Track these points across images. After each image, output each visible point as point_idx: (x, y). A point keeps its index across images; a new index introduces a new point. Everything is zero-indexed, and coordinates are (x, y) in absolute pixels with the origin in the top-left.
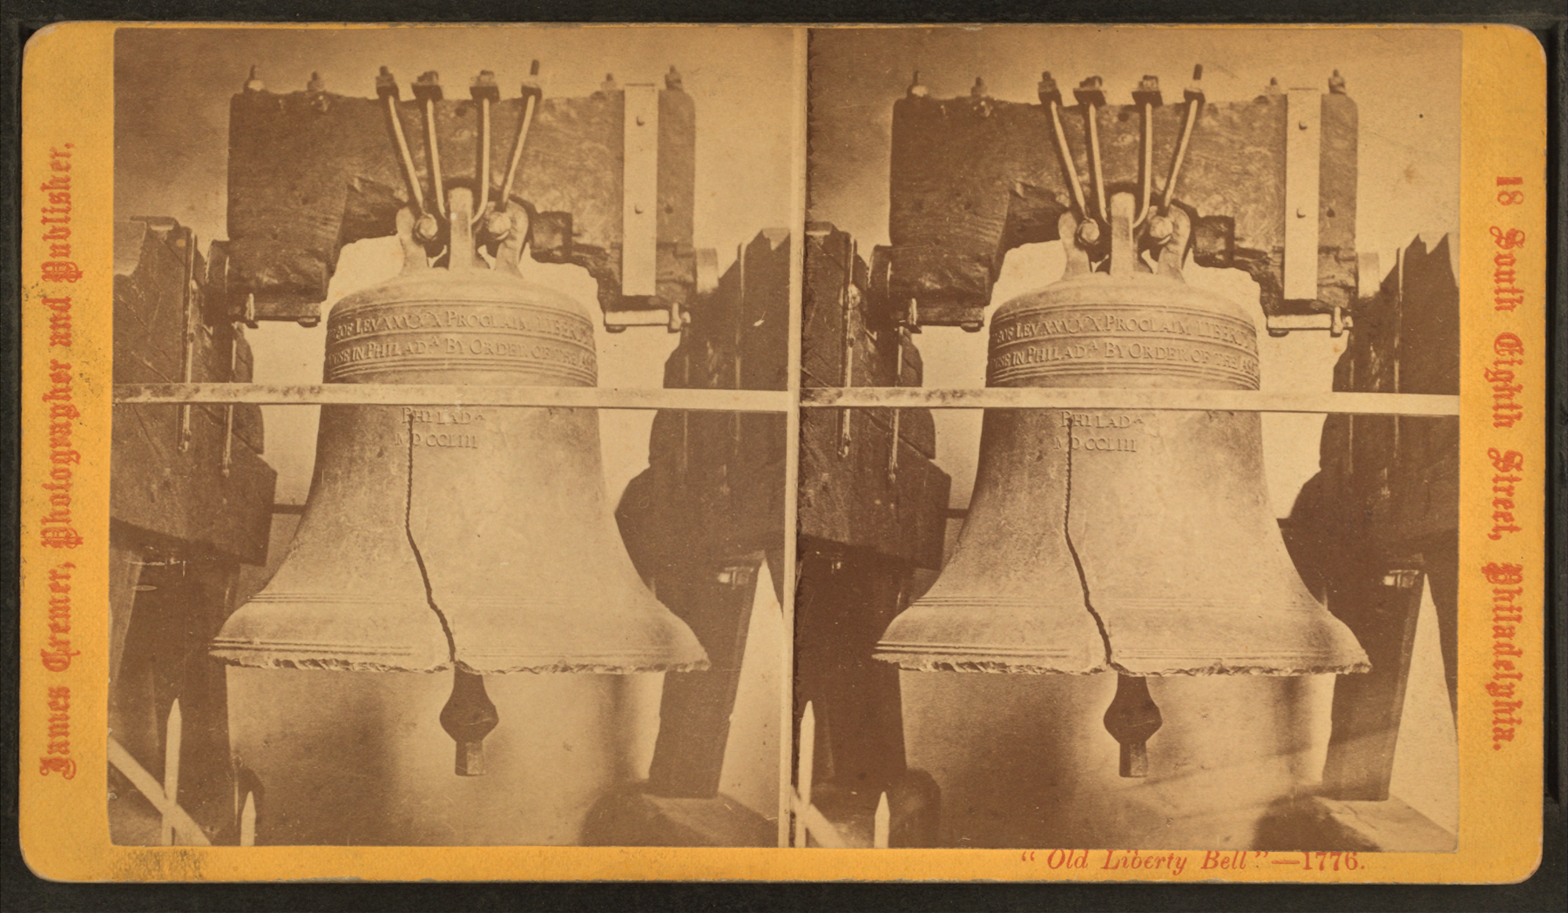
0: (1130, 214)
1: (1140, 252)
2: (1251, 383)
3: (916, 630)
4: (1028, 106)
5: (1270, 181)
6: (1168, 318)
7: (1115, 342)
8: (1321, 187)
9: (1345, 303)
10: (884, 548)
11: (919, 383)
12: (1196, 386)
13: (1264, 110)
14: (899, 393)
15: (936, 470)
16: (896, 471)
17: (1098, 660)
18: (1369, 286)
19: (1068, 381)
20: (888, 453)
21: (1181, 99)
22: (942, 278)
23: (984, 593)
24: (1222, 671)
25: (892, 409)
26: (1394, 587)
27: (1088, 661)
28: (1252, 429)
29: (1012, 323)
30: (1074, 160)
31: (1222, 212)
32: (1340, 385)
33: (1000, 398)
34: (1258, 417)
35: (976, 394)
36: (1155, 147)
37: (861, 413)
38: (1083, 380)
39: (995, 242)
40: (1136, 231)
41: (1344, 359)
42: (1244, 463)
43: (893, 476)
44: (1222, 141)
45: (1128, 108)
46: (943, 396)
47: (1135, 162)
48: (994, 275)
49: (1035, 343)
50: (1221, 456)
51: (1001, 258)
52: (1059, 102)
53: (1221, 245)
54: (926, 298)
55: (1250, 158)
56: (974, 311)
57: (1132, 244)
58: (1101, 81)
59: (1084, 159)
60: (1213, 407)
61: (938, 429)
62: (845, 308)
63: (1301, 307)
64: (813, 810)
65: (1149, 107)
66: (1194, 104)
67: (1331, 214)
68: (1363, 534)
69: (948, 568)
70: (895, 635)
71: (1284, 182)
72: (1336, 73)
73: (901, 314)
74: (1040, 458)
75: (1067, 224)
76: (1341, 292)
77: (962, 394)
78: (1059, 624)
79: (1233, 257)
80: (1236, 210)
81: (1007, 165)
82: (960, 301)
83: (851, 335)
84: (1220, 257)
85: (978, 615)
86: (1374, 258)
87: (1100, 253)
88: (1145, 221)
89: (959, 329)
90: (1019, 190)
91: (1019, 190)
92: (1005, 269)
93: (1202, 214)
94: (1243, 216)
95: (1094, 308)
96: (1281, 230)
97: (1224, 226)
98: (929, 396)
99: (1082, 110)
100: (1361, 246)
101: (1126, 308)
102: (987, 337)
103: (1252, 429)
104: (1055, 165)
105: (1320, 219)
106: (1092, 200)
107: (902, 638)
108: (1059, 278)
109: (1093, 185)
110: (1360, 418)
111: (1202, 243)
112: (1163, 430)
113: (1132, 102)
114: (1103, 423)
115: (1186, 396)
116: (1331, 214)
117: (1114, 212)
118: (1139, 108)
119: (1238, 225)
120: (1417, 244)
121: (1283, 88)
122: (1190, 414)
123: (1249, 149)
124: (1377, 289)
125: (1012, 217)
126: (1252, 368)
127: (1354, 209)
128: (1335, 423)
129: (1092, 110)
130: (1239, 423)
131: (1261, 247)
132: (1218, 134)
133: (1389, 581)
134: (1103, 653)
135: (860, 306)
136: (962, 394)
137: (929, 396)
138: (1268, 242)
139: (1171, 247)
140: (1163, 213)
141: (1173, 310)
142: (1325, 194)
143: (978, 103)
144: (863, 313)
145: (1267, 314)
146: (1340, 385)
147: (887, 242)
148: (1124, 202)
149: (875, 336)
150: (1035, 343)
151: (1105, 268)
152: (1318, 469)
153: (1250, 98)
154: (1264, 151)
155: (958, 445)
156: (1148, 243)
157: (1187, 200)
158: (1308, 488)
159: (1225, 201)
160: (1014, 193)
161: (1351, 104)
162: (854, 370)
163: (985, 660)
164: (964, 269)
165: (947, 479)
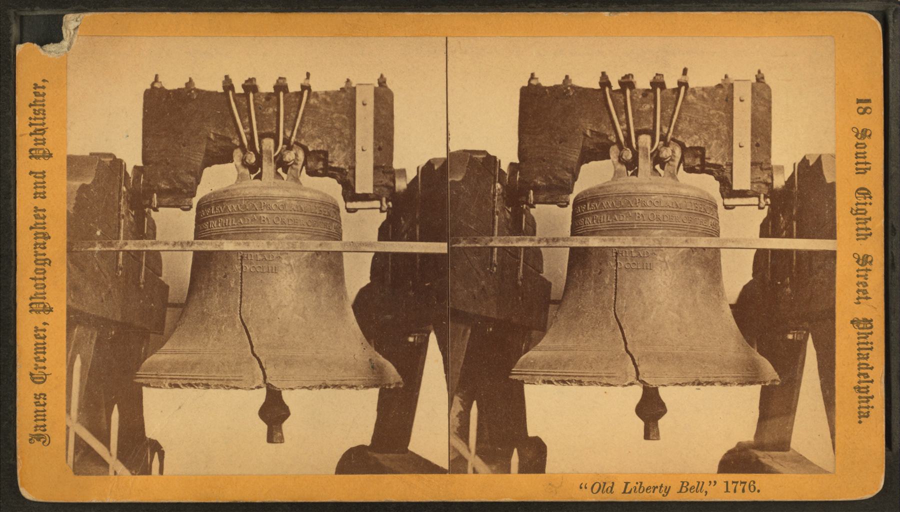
0: (649, 147)
1: (654, 164)
2: (714, 232)
3: (533, 364)
4: (593, 90)
5: (724, 128)
6: (670, 199)
7: (641, 212)
8: (752, 131)
9: (766, 191)
10: (515, 320)
11: (534, 234)
12: (686, 235)
13: (721, 92)
14: (523, 240)
15: (543, 279)
16: (521, 280)
17: (632, 379)
18: (779, 182)
19: (616, 233)
20: (517, 270)
21: (677, 86)
22: (547, 179)
23: (570, 344)
24: (699, 384)
25: (520, 247)
26: (792, 340)
27: (626, 379)
28: (715, 257)
29: (584, 202)
30: (618, 118)
31: (698, 144)
32: (764, 234)
33: (577, 242)
34: (719, 252)
35: (564, 239)
36: (662, 111)
37: (502, 249)
38: (624, 232)
39: (576, 161)
40: (652, 155)
41: (765, 220)
42: (711, 275)
43: (520, 283)
44: (699, 107)
45: (648, 90)
46: (547, 241)
47: (651, 119)
48: (575, 178)
49: (596, 213)
50: (698, 272)
51: (578, 170)
52: (610, 87)
53: (698, 162)
54: (537, 189)
55: (713, 115)
56: (564, 197)
57: (650, 162)
58: (632, 76)
59: (624, 117)
60: (694, 246)
61: (544, 257)
62: (494, 195)
63: (742, 194)
64: (477, 458)
65: (658, 90)
66: (683, 89)
67: (758, 145)
68: (779, 314)
69: (551, 331)
70: (522, 366)
71: (732, 128)
72: (759, 72)
73: (524, 199)
74: (600, 273)
75: (614, 151)
76: (763, 186)
77: (558, 240)
78: (612, 360)
79: (704, 168)
80: (706, 143)
81: (582, 120)
82: (556, 191)
83: (497, 209)
84: (697, 168)
85: (566, 355)
86: (781, 169)
87: (632, 166)
88: (657, 149)
89: (555, 206)
90: (588, 133)
91: (588, 133)
92: (580, 175)
93: (687, 146)
94: (709, 147)
95: (629, 195)
96: (731, 154)
97: (699, 152)
98: (540, 241)
99: (622, 91)
100: (775, 161)
101: (647, 195)
102: (571, 210)
103: (715, 257)
104: (608, 120)
105: (752, 148)
106: (628, 138)
107: (526, 367)
108: (610, 179)
109: (628, 130)
110: (774, 251)
111: (686, 161)
112: (667, 258)
113: (650, 88)
114: (634, 254)
115: (680, 241)
116: (758, 145)
117: (640, 145)
118: (654, 90)
119: (707, 151)
120: (804, 161)
121: (733, 77)
122: (682, 250)
123: (712, 112)
124: (784, 184)
125: (583, 148)
126: (716, 225)
127: (770, 142)
128: (761, 255)
129: (628, 92)
130: (709, 255)
131: (720, 162)
132: (696, 104)
133: (790, 337)
134: (635, 375)
135: (502, 194)
136: (558, 240)
137: (540, 241)
138: (724, 160)
139: (671, 163)
140: (666, 145)
141: (672, 195)
142: (754, 133)
143: (566, 88)
144: (504, 199)
145: (723, 198)
146: (764, 234)
147: (518, 162)
148: (645, 140)
149: (510, 210)
150: (596, 213)
151: (635, 173)
152: (751, 278)
153: (714, 84)
154: (722, 113)
155: (556, 266)
156: (658, 160)
157: (680, 139)
158: (745, 287)
159: (700, 139)
160: (585, 135)
161: (768, 87)
162: (499, 227)
163: (570, 378)
164: (559, 175)
165: (550, 284)
